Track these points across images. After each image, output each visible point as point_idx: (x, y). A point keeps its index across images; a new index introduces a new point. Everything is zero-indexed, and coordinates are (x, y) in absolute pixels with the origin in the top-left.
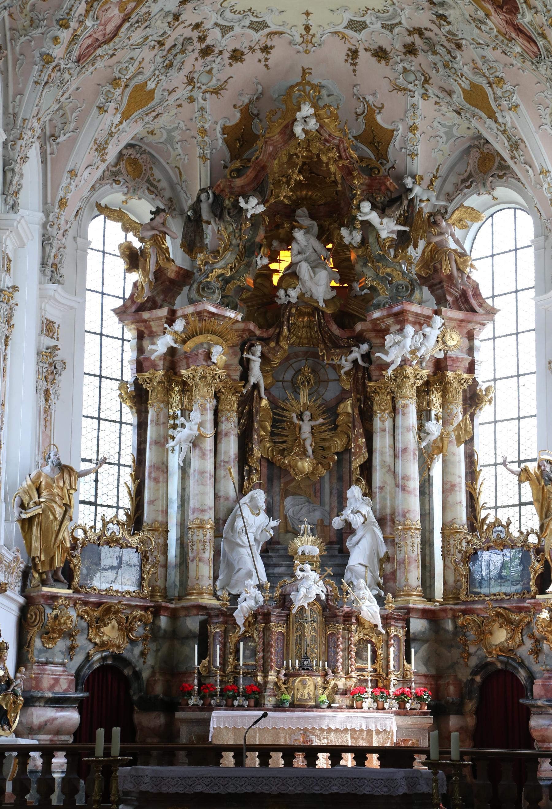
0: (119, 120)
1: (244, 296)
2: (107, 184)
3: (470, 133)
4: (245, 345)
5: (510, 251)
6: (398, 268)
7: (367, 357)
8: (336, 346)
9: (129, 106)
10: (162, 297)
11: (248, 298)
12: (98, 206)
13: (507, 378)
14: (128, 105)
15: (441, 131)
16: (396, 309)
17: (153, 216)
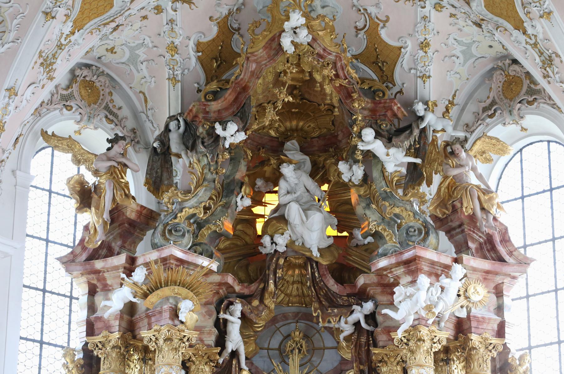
0: (70, 29)
1: (222, 246)
2: (55, 109)
3: (492, 53)
4: (222, 303)
5: (544, 191)
6: (408, 207)
7: (371, 318)
8: (333, 305)
9: (83, 14)
10: (119, 243)
11: (226, 248)
12: (44, 133)
13: (545, 345)
14: (82, 12)
15: (458, 50)
16: (407, 255)
17: (110, 145)
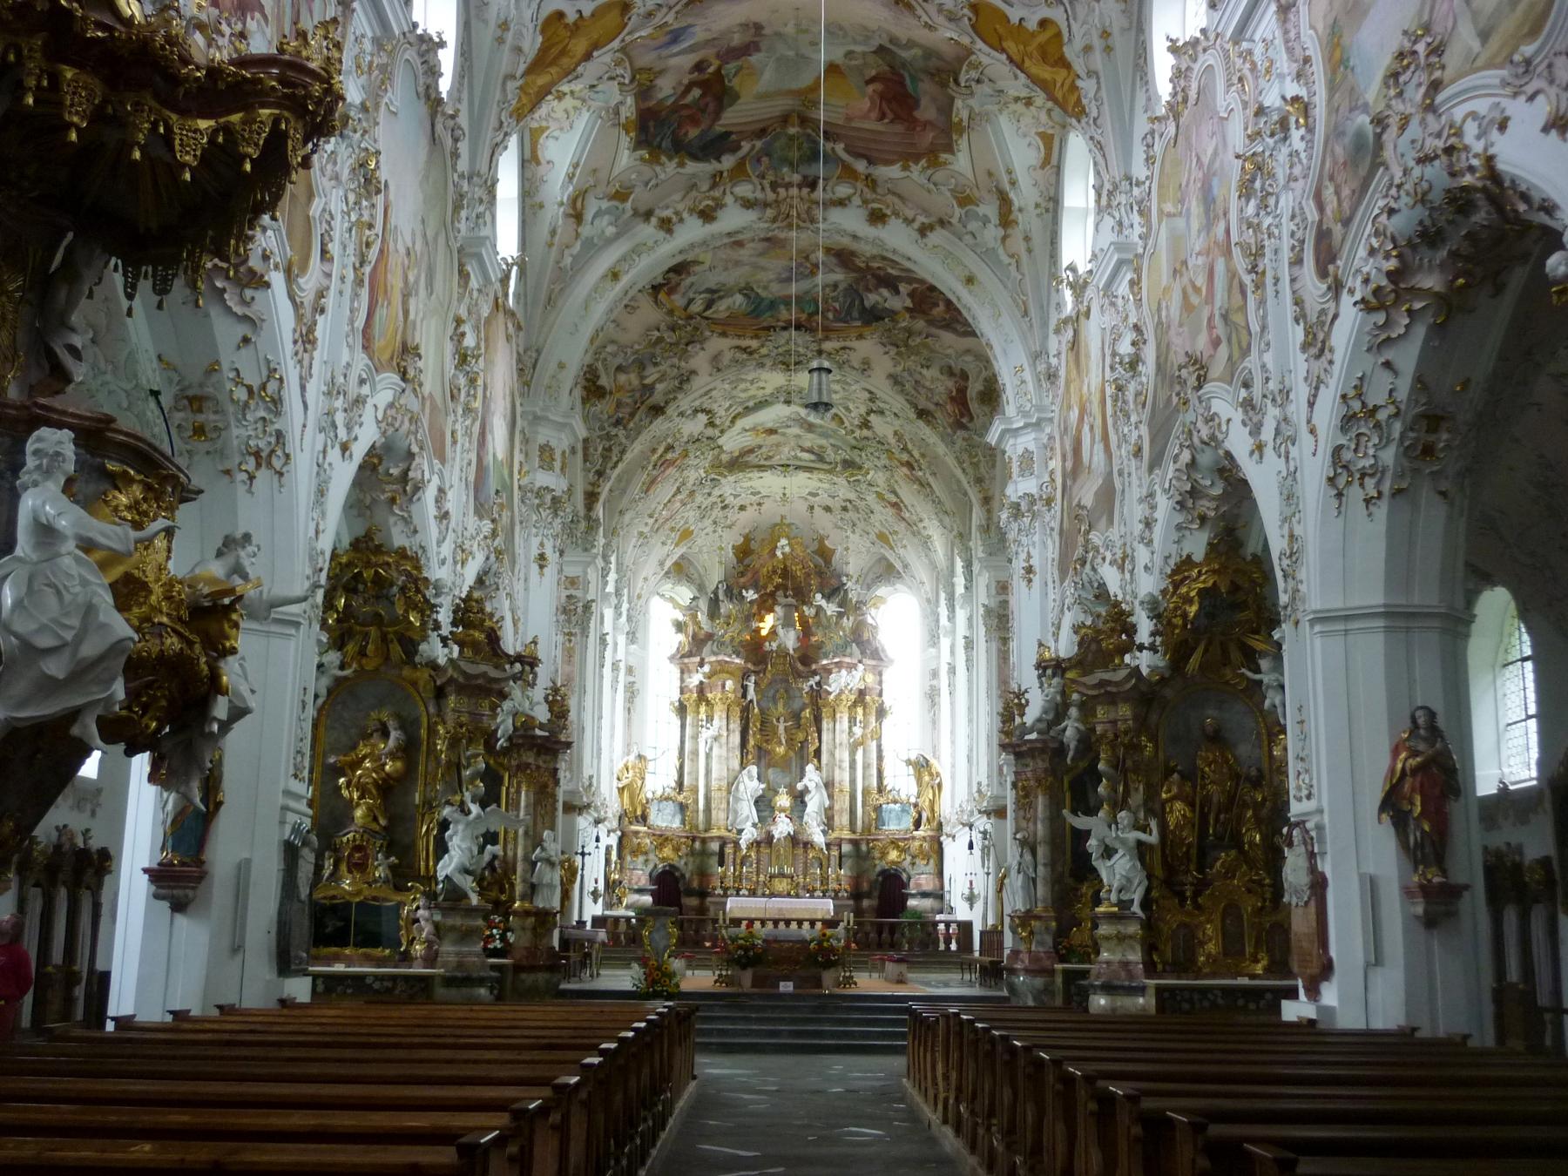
4: (745, 675)
7: (818, 684)
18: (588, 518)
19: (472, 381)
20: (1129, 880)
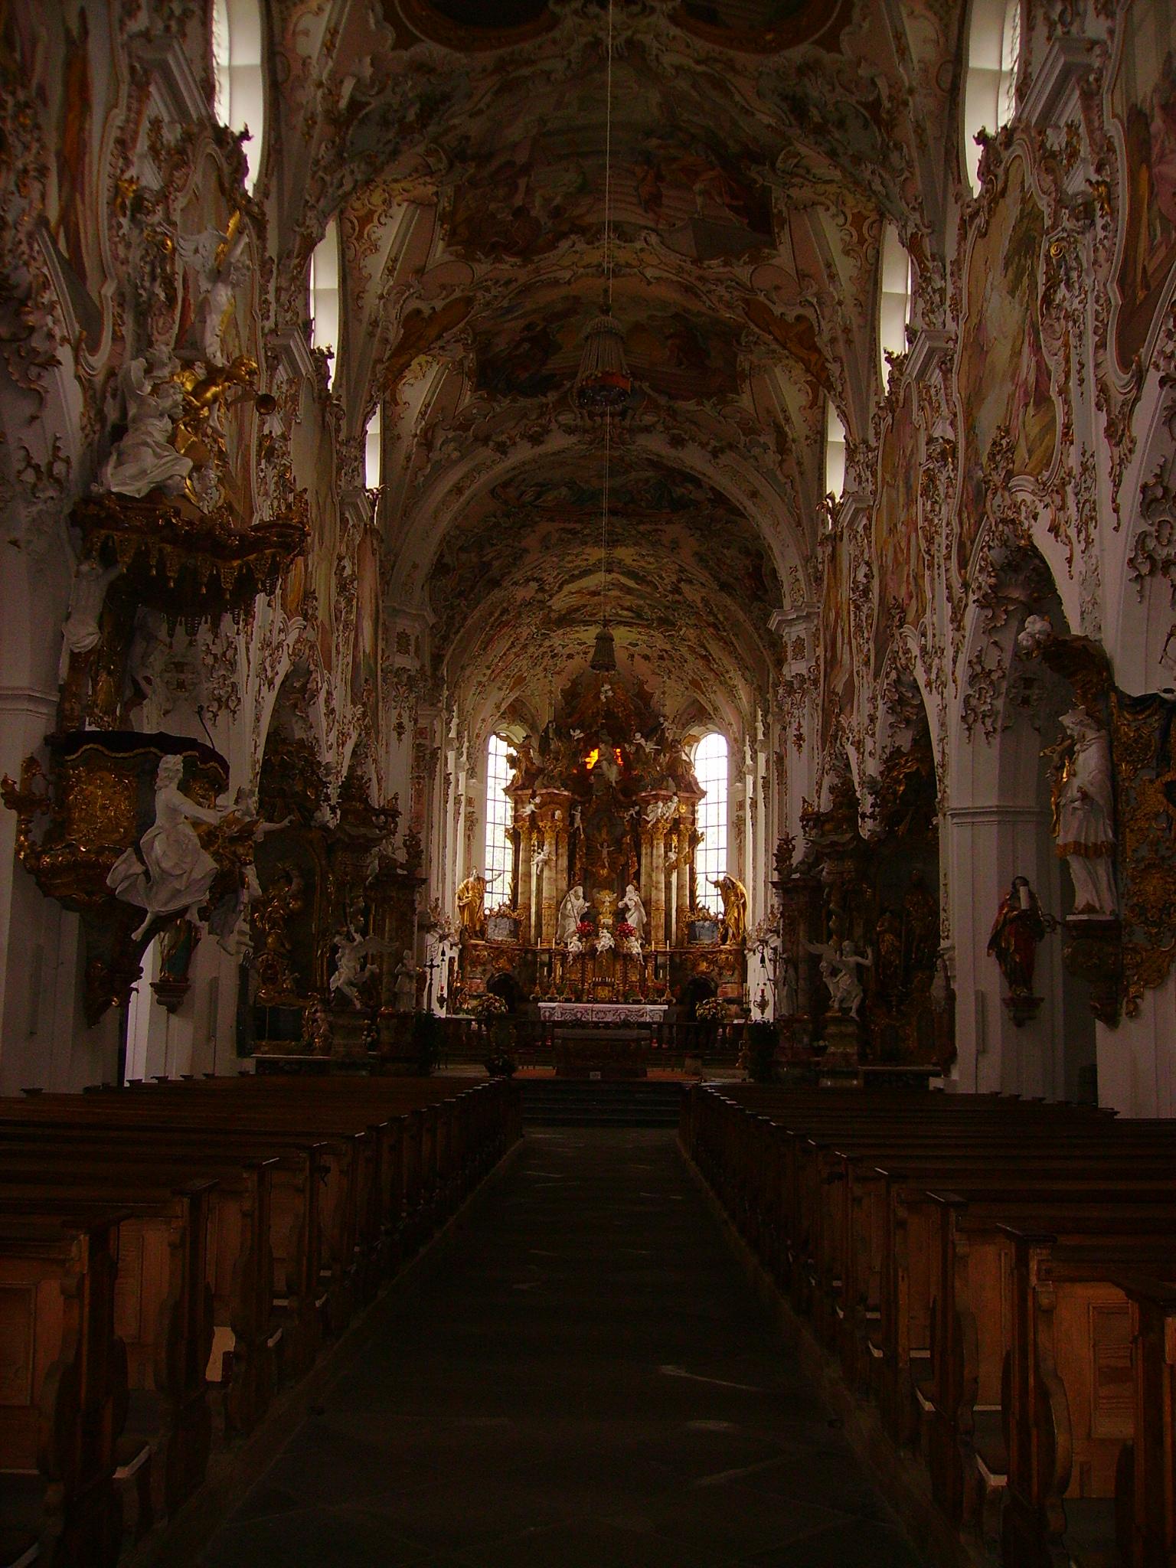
18: (434, 676)
19: (349, 601)
20: (849, 993)
